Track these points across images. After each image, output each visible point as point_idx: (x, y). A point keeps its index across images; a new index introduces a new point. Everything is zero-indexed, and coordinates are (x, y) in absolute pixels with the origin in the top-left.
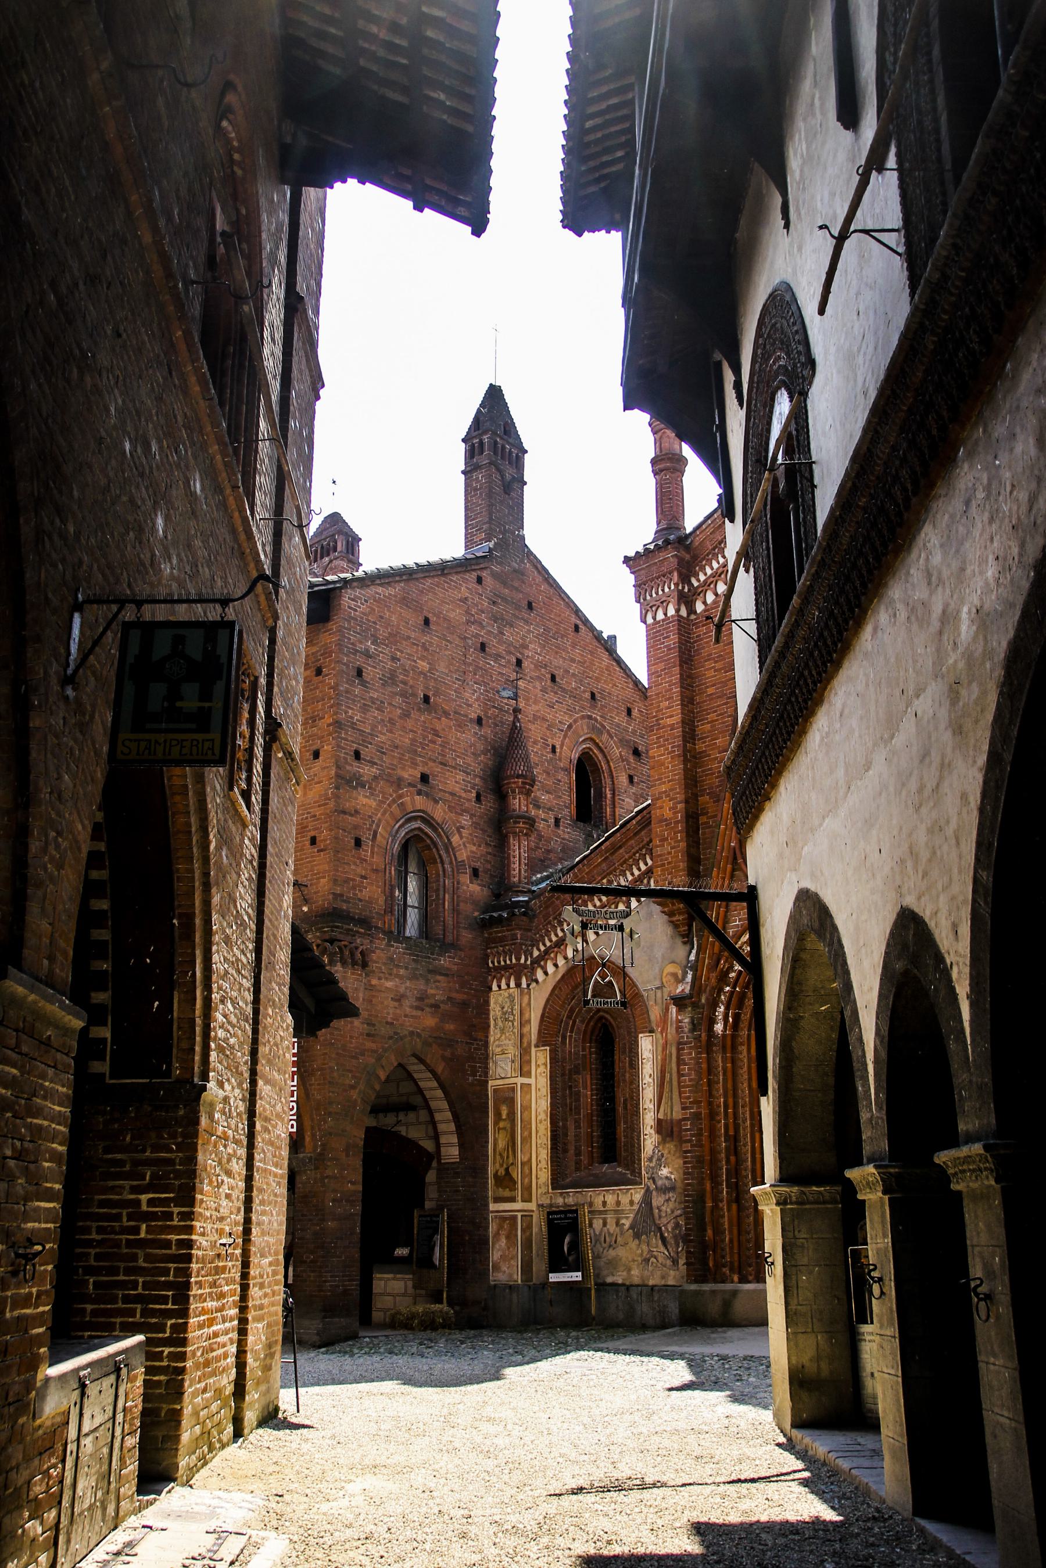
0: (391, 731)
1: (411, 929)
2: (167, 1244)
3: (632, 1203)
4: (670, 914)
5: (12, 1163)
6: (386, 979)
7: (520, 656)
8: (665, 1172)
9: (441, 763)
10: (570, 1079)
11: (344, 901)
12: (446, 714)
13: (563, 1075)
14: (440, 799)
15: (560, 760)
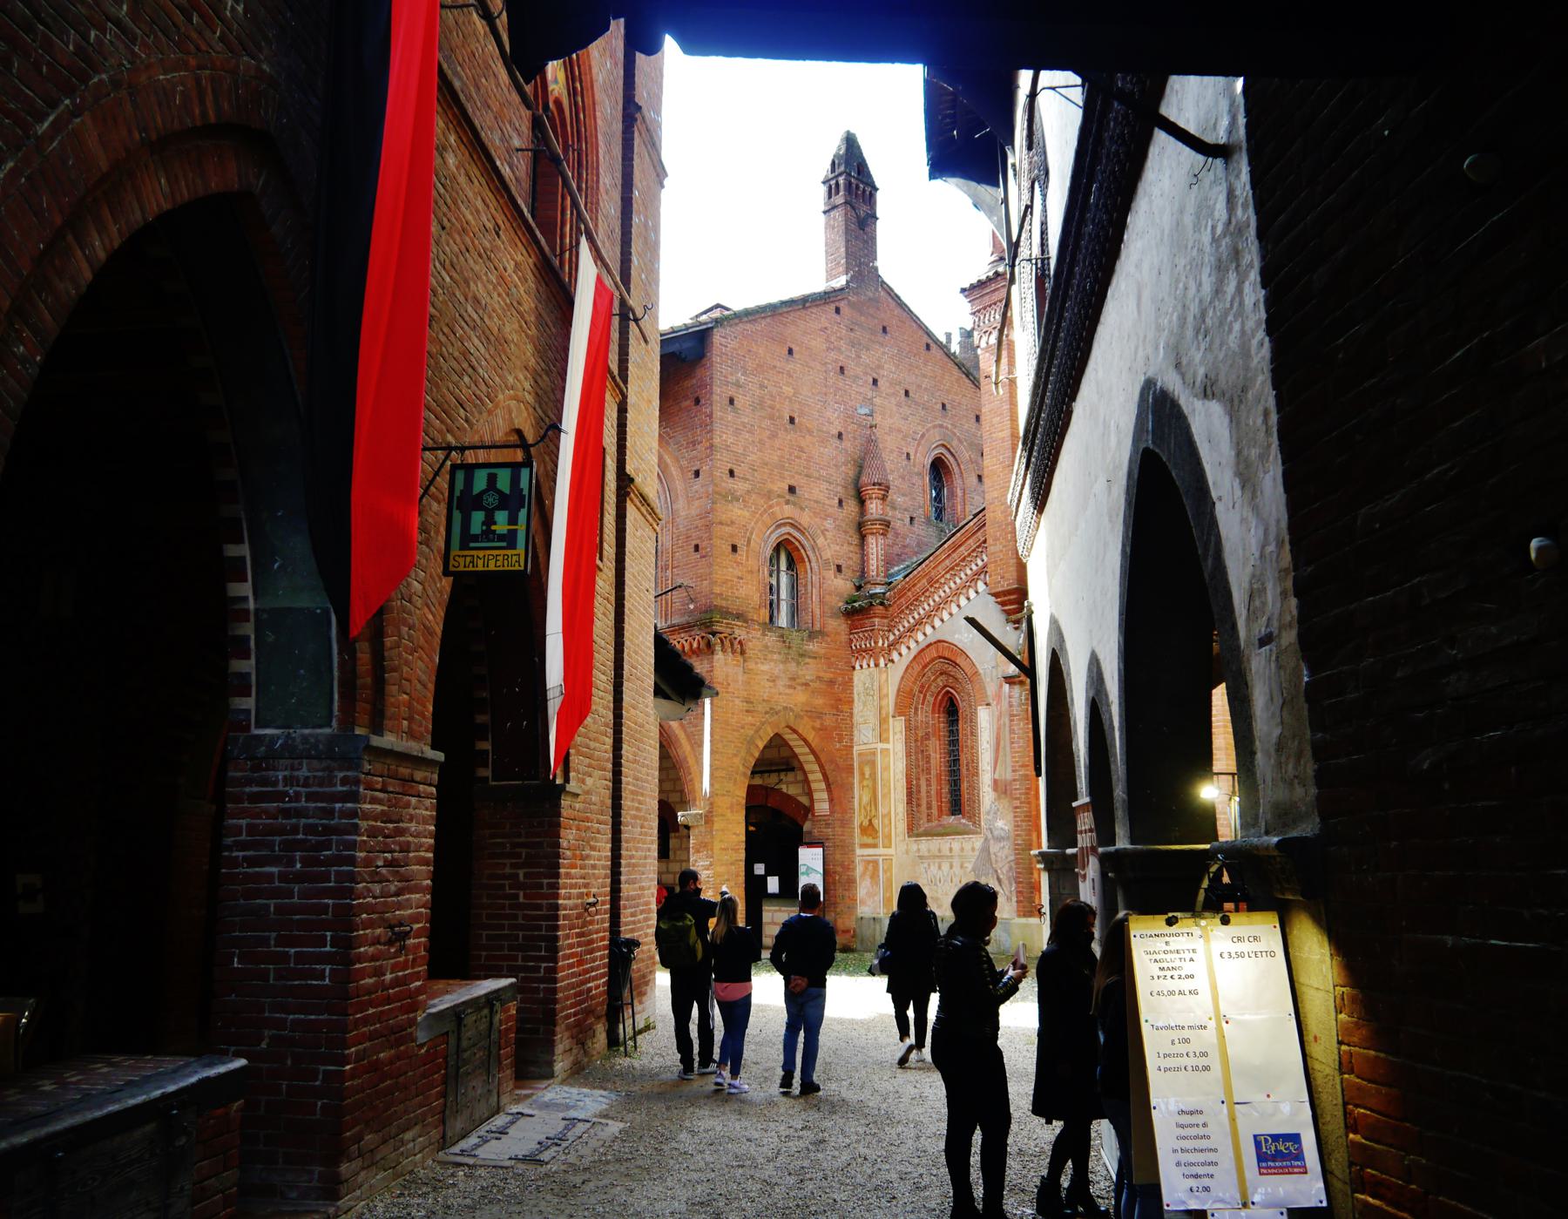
0: (761, 451)
1: (783, 620)
2: (539, 907)
3: (973, 849)
4: (1003, 604)
5: (384, 871)
6: (762, 663)
7: (875, 376)
8: (1000, 824)
9: (807, 476)
10: (922, 743)
11: (724, 599)
12: (810, 432)
13: (916, 741)
15: (914, 466)
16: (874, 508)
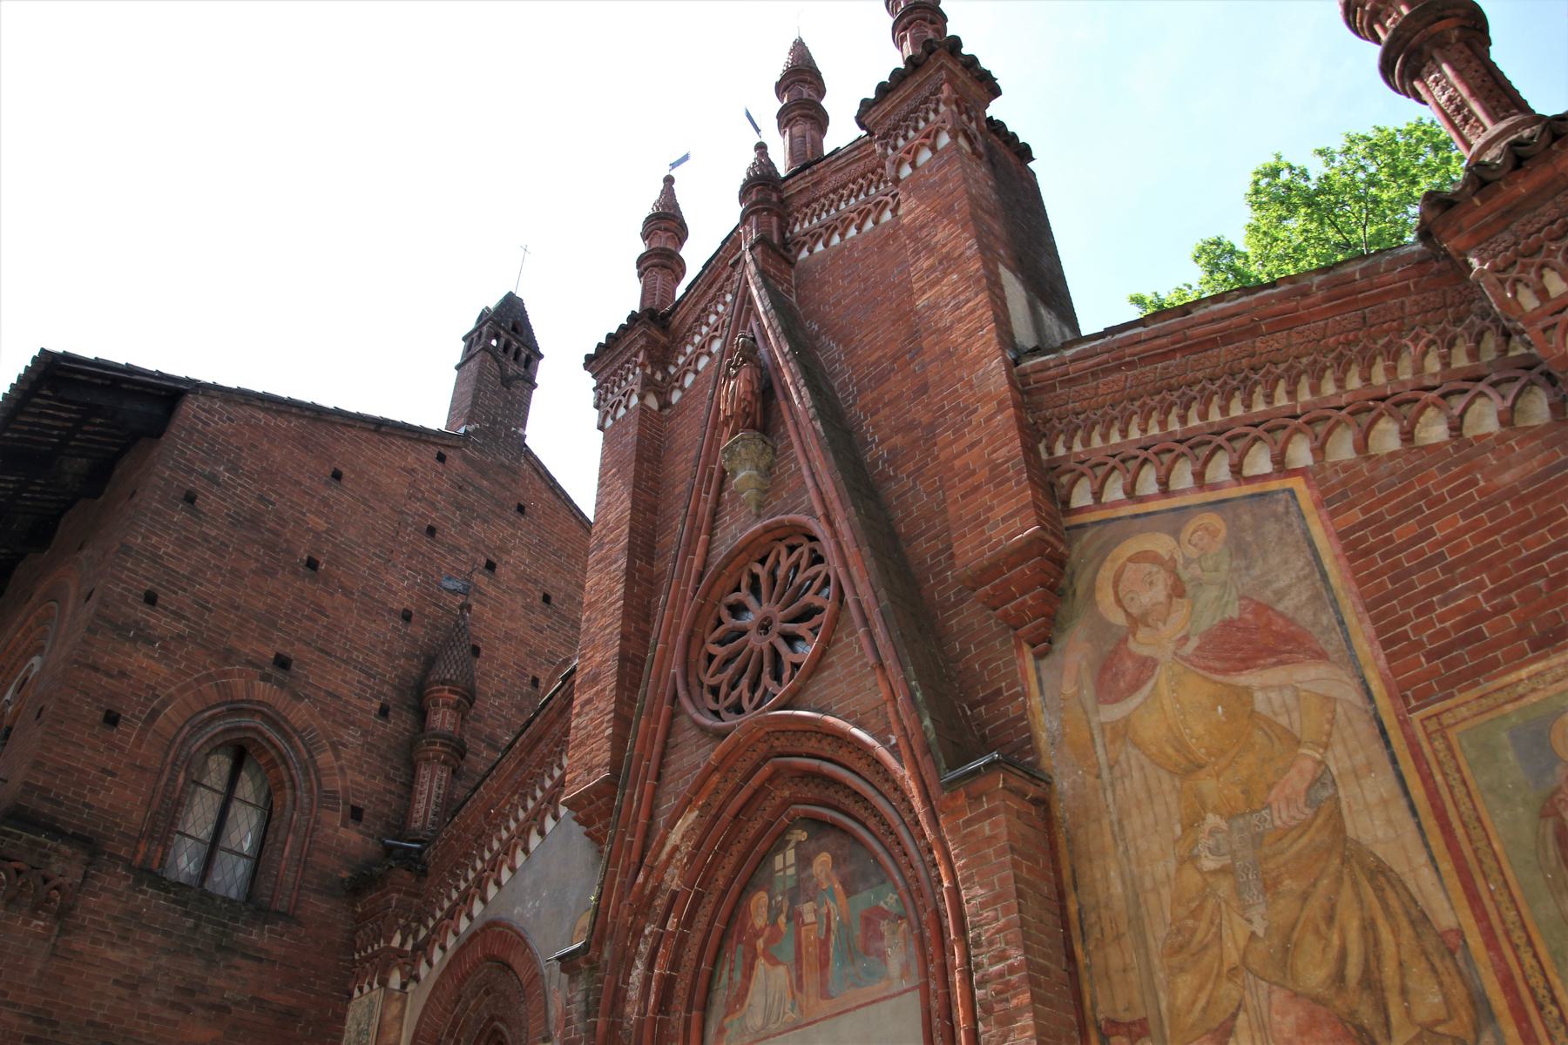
6: (113, 945)
9: (322, 651)
12: (347, 593)
14: (307, 696)
16: (442, 720)
